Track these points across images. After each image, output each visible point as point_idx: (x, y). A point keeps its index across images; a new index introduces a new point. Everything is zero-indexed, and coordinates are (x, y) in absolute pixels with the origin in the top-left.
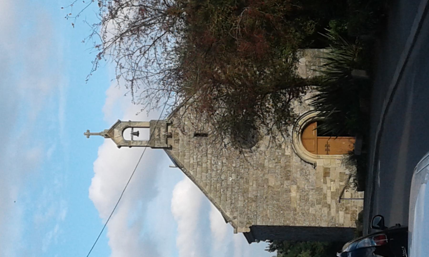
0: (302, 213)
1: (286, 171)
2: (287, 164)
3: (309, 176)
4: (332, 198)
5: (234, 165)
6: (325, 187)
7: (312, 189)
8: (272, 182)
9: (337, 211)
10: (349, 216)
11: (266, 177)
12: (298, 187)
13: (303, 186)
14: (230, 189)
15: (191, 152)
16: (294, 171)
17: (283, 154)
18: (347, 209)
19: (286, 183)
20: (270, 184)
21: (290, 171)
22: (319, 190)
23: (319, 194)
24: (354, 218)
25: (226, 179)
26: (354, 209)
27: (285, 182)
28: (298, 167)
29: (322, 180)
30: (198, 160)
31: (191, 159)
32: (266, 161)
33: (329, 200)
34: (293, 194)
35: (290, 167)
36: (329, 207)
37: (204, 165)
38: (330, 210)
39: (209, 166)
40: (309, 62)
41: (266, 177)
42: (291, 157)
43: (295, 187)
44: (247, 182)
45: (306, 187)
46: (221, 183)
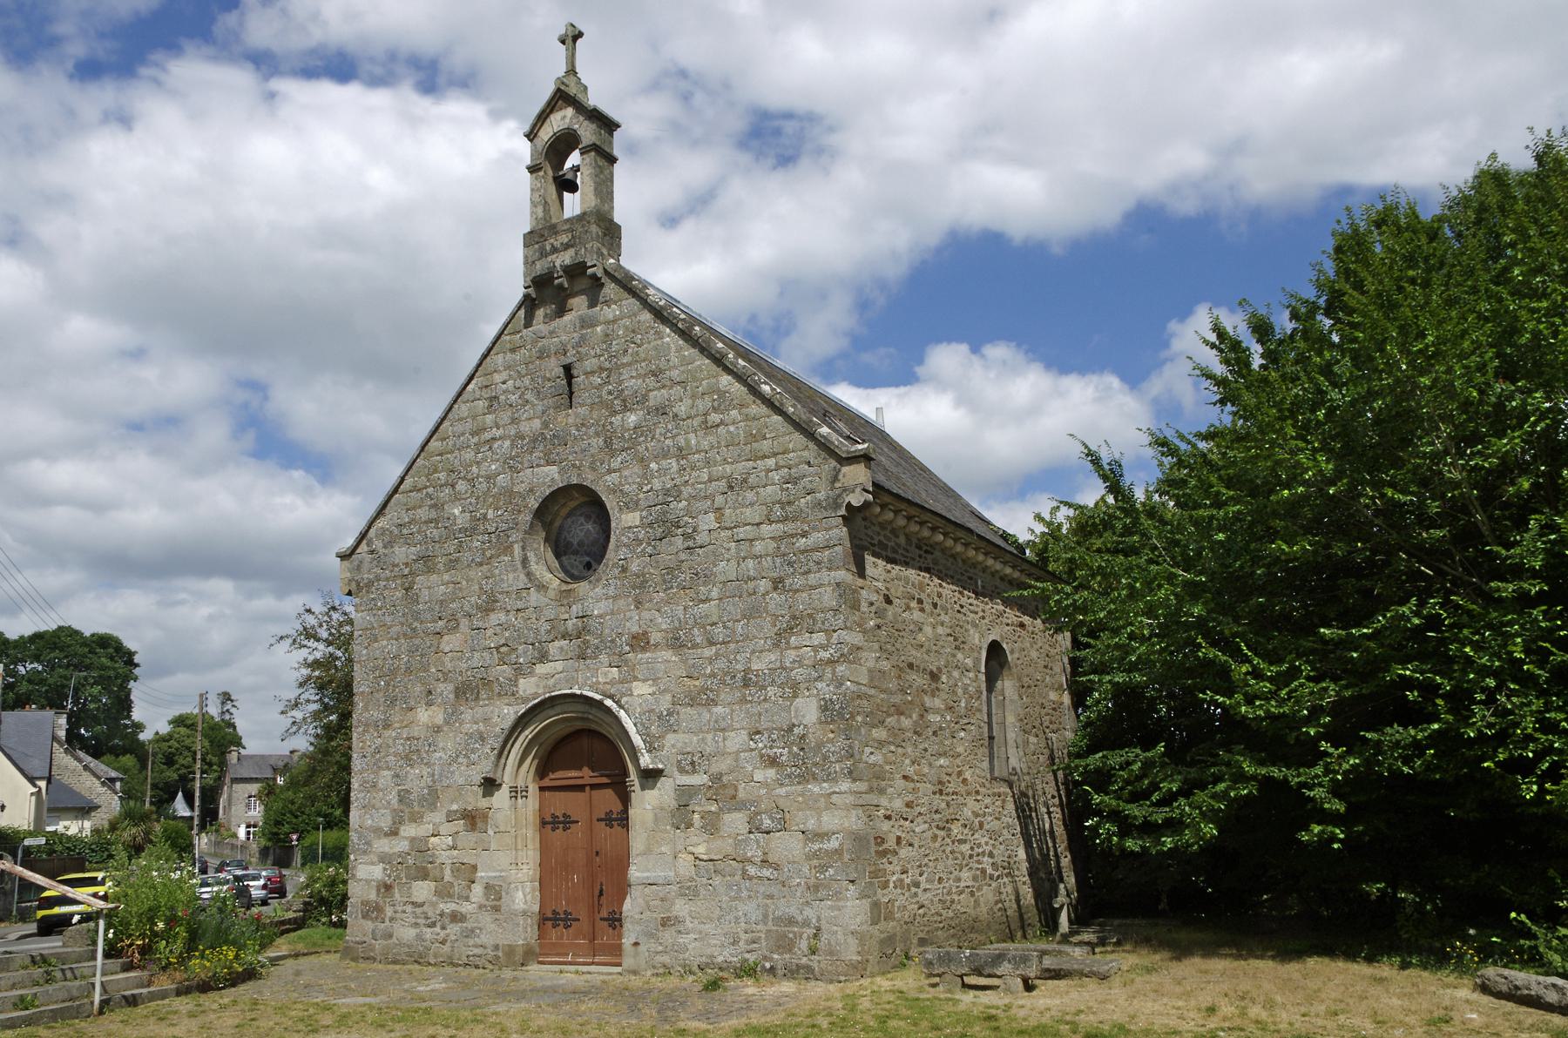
0: (381, 746)
1: (477, 686)
3: (465, 761)
4: (413, 840)
5: (490, 514)
6: (439, 816)
7: (433, 775)
8: (450, 642)
9: (384, 859)
10: (373, 896)
12: (438, 730)
13: (441, 745)
14: (433, 515)
15: (523, 370)
17: (519, 671)
18: (388, 888)
19: (446, 689)
21: (477, 698)
22: (432, 798)
23: (422, 799)
24: (368, 911)
25: (456, 498)
26: (389, 912)
27: (451, 687)
29: (455, 807)
30: (502, 398)
31: (504, 375)
32: (502, 617)
33: (409, 830)
34: (424, 715)
35: (488, 699)
36: (394, 833)
37: (489, 418)
38: (386, 835)
39: (487, 436)
40: (803, 737)
41: (464, 622)
44: (452, 564)
46: (446, 484)
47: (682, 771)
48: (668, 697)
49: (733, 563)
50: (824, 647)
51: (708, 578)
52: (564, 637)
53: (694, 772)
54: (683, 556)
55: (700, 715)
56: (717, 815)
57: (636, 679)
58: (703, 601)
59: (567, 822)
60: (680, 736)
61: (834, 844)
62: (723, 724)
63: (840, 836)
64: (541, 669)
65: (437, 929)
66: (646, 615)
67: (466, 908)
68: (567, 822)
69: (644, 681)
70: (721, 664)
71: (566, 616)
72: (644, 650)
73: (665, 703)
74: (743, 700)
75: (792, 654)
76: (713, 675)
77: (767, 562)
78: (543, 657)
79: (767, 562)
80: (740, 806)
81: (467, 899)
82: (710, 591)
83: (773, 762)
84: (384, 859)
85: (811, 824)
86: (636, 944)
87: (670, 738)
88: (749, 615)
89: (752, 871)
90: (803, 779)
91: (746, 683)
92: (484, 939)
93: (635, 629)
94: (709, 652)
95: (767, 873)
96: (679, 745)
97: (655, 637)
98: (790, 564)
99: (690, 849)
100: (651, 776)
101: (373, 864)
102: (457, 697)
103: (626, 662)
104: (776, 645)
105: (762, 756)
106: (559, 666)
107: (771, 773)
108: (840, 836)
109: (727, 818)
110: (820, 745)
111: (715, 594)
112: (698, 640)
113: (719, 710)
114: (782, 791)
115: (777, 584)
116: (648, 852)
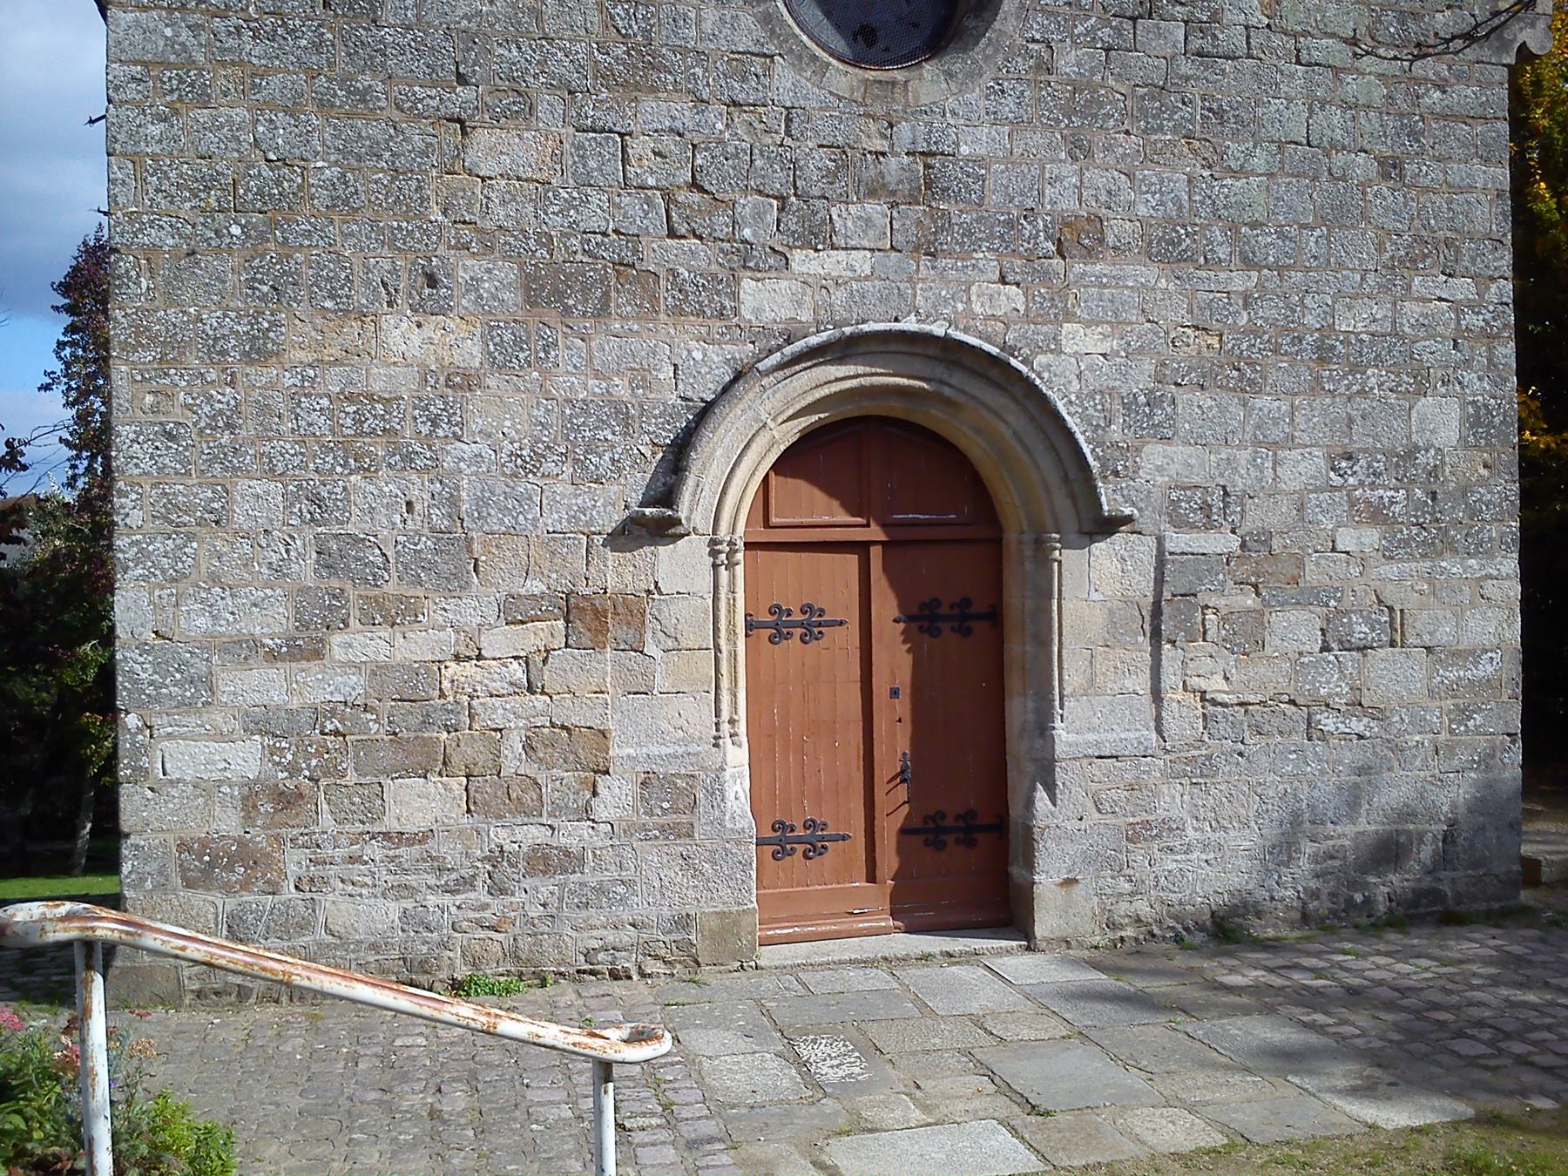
0: (236, 410)
1: (604, 279)
2: (667, 298)
7: (454, 501)
9: (260, 723)
10: (228, 823)
11: (548, 106)
13: (477, 423)
16: (606, 348)
17: (744, 258)
18: (287, 800)
20: (482, 137)
21: (602, 311)
24: (211, 865)
26: (294, 862)
27: (507, 272)
28: (642, 378)
29: (536, 586)
32: (682, 111)
38: (273, 656)
40: (1434, 472)
41: (548, 106)
42: (717, 325)
43: (470, 353)
45: (468, 450)
47: (1180, 523)
48: (1149, 366)
49: (1300, 107)
50: (1475, 307)
51: (1249, 128)
52: (872, 193)
53: (1209, 526)
54: (1186, 67)
55: (1223, 410)
56: (1257, 618)
57: (1070, 317)
58: (1235, 174)
59: (813, 625)
60: (1178, 451)
61: (1486, 669)
62: (1276, 434)
63: (1497, 657)
64: (803, 261)
65: (480, 895)
66: (1098, 178)
67: (574, 835)
68: (813, 625)
69: (1088, 324)
70: (1269, 311)
71: (881, 145)
72: (1090, 254)
73: (1141, 378)
74: (1316, 386)
75: (1412, 309)
76: (1253, 331)
77: (1369, 122)
78: (818, 236)
79: (1369, 122)
80: (1309, 597)
81: (586, 813)
82: (1249, 155)
83: (1377, 514)
84: (260, 723)
85: (1444, 633)
86: (1070, 882)
87: (1154, 454)
88: (1334, 218)
89: (1328, 722)
90: (1431, 550)
91: (1324, 355)
92: (640, 906)
93: (1068, 204)
94: (1241, 281)
95: (1358, 726)
96: (1173, 469)
97: (1119, 229)
98: (1414, 135)
99: (1195, 682)
100: (1107, 526)
101: (220, 737)
102: (531, 301)
103: (1046, 276)
104: (1384, 288)
105: (1353, 503)
106: (862, 262)
107: (1371, 537)
108: (1497, 657)
109: (1279, 620)
110: (1465, 490)
111: (1259, 161)
112: (1222, 252)
113: (1263, 402)
114: (1391, 570)
115: (1391, 168)
116: (1092, 687)
